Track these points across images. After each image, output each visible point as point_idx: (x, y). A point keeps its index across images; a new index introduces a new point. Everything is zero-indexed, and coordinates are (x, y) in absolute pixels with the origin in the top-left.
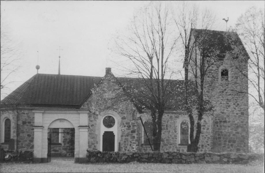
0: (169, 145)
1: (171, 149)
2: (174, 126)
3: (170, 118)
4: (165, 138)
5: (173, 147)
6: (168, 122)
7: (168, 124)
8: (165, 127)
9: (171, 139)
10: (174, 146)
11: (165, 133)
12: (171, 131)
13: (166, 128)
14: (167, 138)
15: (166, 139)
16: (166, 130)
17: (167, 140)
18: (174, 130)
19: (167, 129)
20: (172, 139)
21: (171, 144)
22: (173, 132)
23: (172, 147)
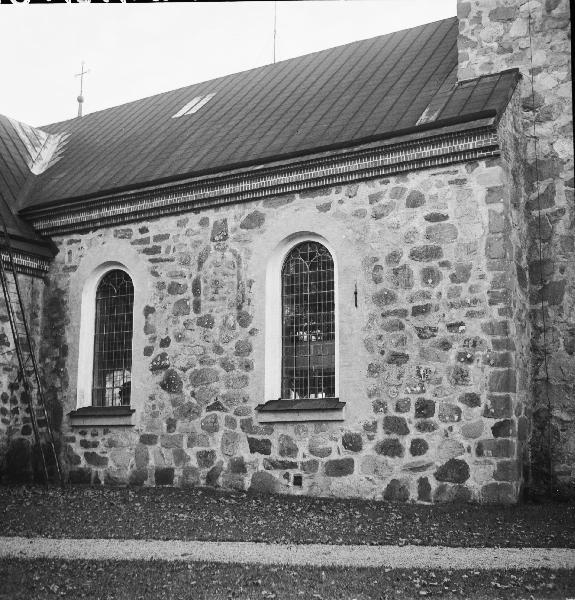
0: (204, 414)
1: (219, 436)
2: (235, 279)
3: (213, 240)
4: (184, 370)
5: (231, 422)
6: (200, 263)
7: (201, 273)
8: (189, 293)
9: (217, 372)
10: (231, 414)
11: (188, 333)
12: (218, 321)
13: (190, 303)
14: (198, 367)
15: (190, 371)
16: (192, 315)
17: (198, 379)
18: (235, 311)
19: (197, 306)
20: (222, 372)
21: (217, 406)
22: (232, 320)
23: (221, 422)
